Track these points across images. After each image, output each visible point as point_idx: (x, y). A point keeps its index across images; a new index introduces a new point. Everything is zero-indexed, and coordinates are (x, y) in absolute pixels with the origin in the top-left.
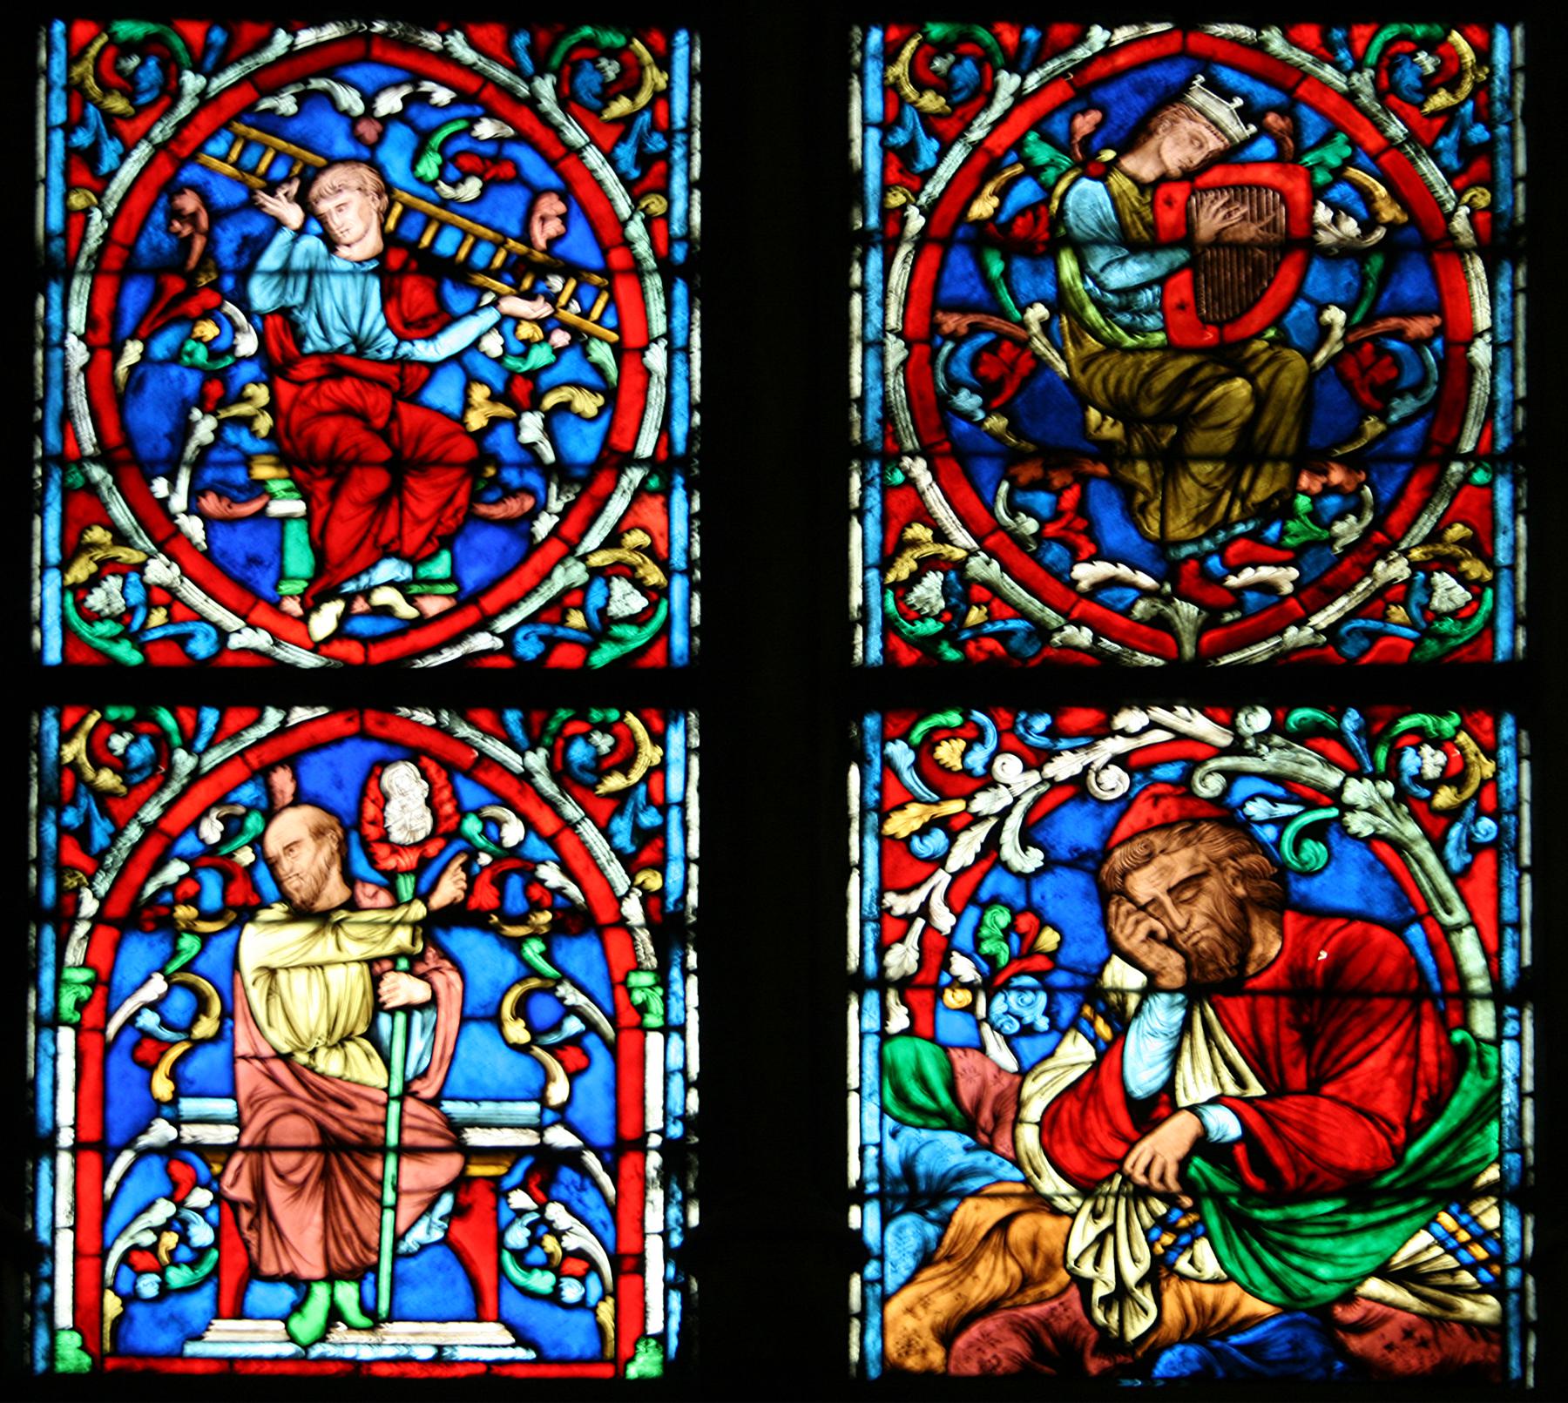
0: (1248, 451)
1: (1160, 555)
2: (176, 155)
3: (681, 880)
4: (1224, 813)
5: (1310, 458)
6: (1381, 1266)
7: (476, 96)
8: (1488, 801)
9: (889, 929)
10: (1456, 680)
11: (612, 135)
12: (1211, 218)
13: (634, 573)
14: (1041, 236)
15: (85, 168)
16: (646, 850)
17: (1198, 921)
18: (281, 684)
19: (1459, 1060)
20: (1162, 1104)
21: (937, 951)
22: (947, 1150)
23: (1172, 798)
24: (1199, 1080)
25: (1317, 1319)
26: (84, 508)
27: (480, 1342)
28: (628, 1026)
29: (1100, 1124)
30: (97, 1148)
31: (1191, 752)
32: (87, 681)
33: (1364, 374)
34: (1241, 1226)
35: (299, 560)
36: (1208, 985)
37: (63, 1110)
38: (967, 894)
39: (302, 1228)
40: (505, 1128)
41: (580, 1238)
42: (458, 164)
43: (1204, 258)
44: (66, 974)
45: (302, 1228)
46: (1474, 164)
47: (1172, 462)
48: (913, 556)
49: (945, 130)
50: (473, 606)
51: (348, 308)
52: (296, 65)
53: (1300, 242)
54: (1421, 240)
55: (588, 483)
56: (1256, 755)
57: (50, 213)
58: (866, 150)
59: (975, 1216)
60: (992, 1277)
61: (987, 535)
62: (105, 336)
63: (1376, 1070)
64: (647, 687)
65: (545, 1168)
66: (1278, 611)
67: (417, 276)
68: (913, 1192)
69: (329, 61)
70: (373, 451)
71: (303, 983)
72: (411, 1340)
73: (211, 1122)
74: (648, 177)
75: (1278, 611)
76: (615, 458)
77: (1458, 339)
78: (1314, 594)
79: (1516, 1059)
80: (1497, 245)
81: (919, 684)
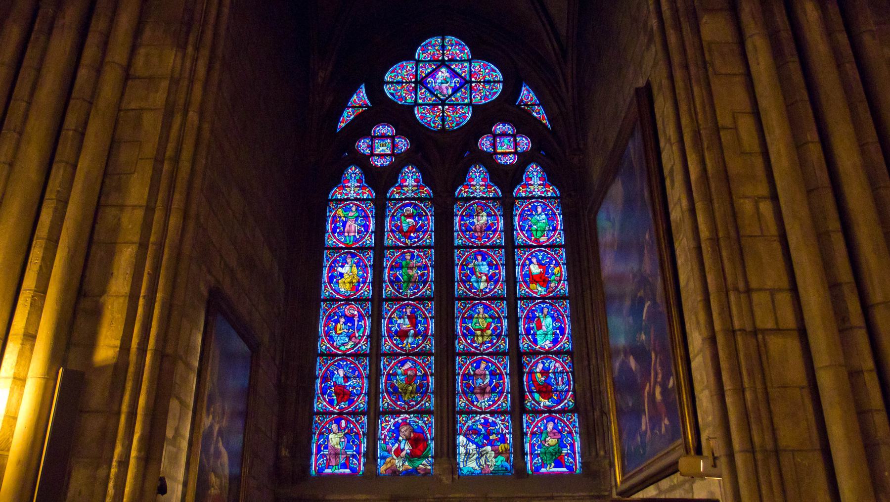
0: (411, 393)
1: (404, 402)
2: (327, 369)
3: (365, 430)
4: (409, 424)
5: (416, 393)
6: (423, 464)
7: (352, 363)
8: (430, 422)
9: (382, 434)
10: (429, 412)
11: (362, 366)
12: (409, 373)
13: (361, 403)
14: (395, 374)
15: (320, 369)
16: (362, 427)
17: (407, 433)
18: (333, 413)
19: (427, 445)
20: (404, 449)
21: (386, 436)
22: (386, 454)
23: (404, 422)
24: (406, 448)
25: (415, 470)
26: (319, 398)
27: (348, 471)
28: (361, 443)
29: (398, 452)
30: (317, 454)
31: (406, 418)
32: (318, 413)
33: (421, 386)
34: (410, 461)
35: (336, 402)
36: (408, 439)
37: (314, 451)
38: (388, 431)
39: (333, 460)
40: (350, 452)
41: (356, 462)
42: (350, 368)
43: (408, 377)
44: (315, 438)
45: (333, 460)
46: (430, 368)
47: (405, 394)
48: (385, 402)
49: (388, 365)
50: (349, 406)
51: (341, 381)
52: (337, 360)
53: (416, 374)
54: (425, 375)
55: (359, 396)
56: (412, 418)
57: (317, 373)
58: (382, 367)
59: (388, 460)
60: (389, 465)
61: (391, 400)
62: (321, 384)
63: (421, 446)
64: (363, 413)
65: (354, 456)
66: (414, 406)
67: (346, 378)
68: (383, 458)
69: (340, 360)
70: (343, 394)
71: (335, 440)
72: (342, 471)
73: (326, 452)
74: (365, 369)
75: (414, 406)
76: (361, 393)
77: (428, 383)
78: (417, 404)
79: (433, 445)
80: (432, 374)
81: (385, 413)
